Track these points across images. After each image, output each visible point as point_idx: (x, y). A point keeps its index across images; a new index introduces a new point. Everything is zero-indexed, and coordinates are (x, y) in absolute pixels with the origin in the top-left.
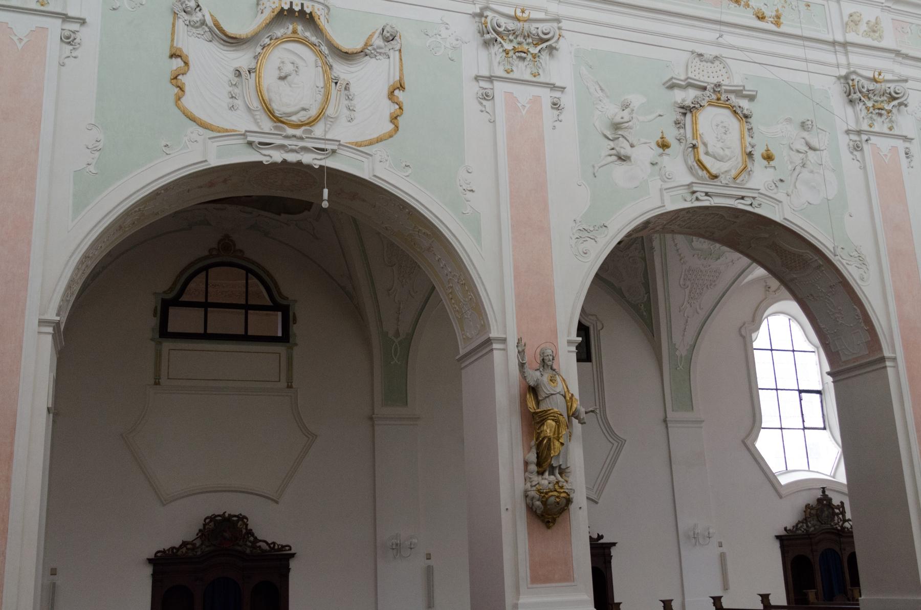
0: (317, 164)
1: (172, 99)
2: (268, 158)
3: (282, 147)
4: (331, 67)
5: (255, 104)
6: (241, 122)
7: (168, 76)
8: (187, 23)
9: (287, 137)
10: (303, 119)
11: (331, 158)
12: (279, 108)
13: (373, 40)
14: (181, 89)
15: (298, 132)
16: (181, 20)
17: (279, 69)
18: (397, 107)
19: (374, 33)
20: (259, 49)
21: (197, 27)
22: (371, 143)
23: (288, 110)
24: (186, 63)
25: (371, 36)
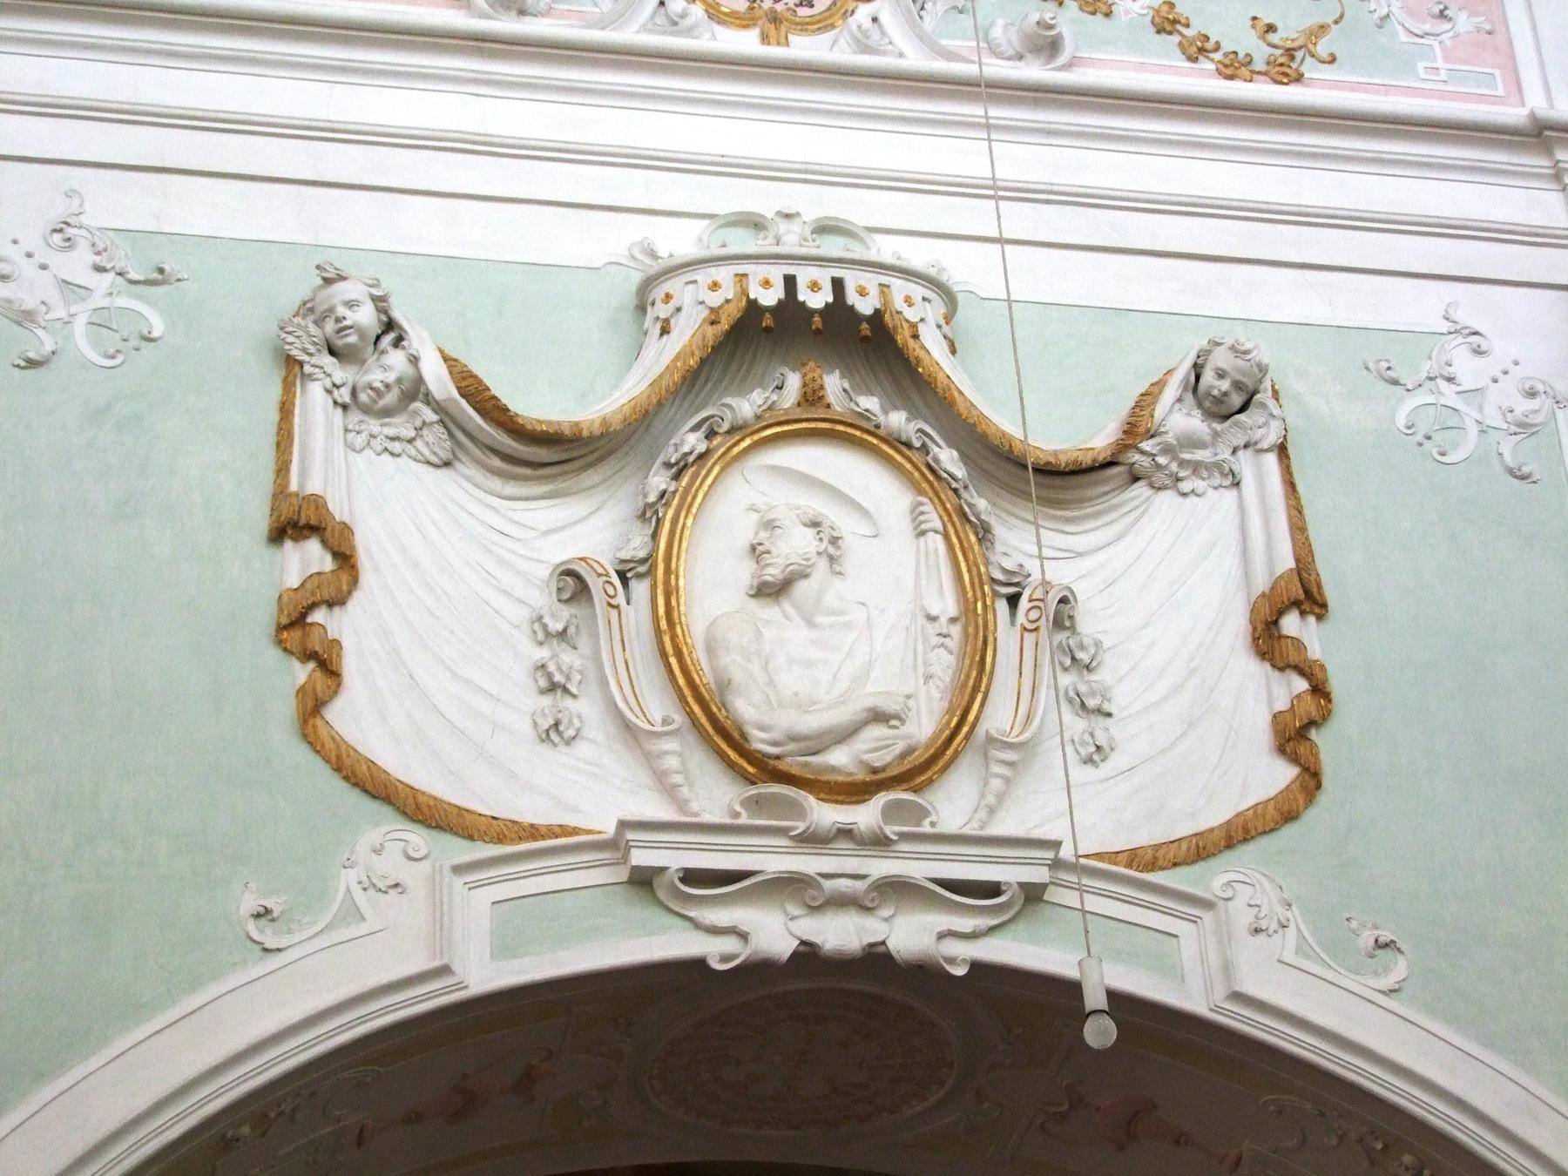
0: (960, 956)
1: (285, 709)
2: (729, 945)
3: (790, 886)
4: (984, 533)
5: (657, 706)
6: (596, 789)
7: (265, 615)
8: (344, 395)
9: (813, 840)
10: (879, 759)
11: (1020, 927)
12: (763, 715)
13: (1159, 412)
14: (326, 663)
15: (865, 816)
16: (316, 391)
17: (756, 552)
18: (1301, 685)
19: (1158, 387)
20: (659, 481)
21: (387, 413)
22: (1200, 849)
24: (345, 559)
25: (1148, 399)
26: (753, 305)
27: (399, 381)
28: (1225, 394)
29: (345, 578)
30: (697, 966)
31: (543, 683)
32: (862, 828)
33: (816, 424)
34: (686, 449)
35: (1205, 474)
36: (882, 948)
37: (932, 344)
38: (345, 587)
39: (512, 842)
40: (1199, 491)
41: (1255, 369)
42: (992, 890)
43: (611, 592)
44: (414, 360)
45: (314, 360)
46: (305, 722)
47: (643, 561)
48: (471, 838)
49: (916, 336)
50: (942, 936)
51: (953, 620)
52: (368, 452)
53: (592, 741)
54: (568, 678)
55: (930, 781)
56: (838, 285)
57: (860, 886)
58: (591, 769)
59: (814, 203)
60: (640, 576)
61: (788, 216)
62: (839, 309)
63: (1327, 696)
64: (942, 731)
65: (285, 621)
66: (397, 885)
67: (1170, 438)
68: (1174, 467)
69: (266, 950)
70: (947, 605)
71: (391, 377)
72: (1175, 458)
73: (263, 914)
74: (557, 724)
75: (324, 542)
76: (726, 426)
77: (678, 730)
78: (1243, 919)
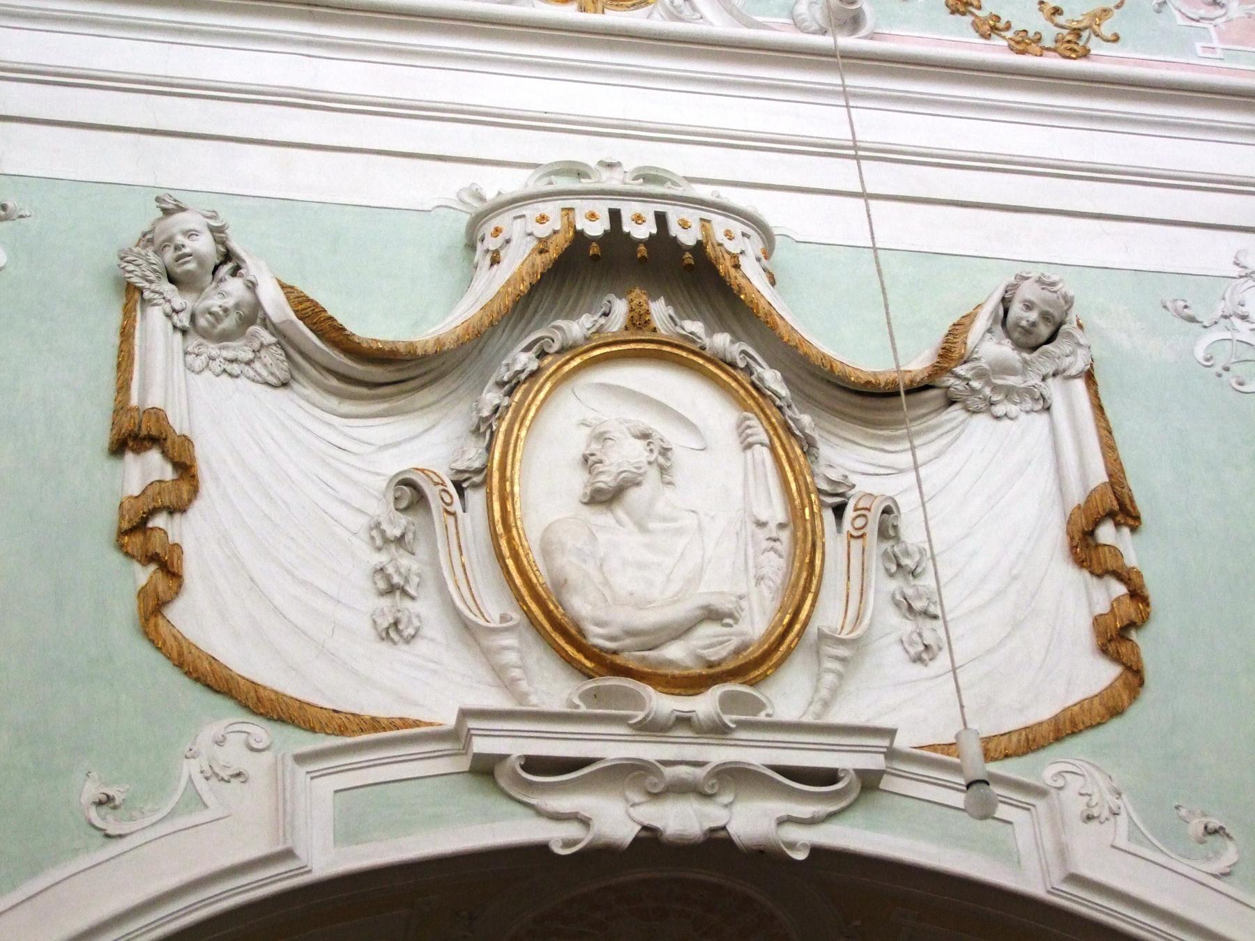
0: (800, 841)
1: (126, 609)
2: (571, 831)
4: (809, 446)
5: (494, 606)
6: (434, 683)
7: (107, 521)
9: (652, 728)
10: (714, 655)
11: (857, 815)
12: (599, 611)
14: (167, 565)
15: (704, 705)
16: (156, 315)
17: (588, 462)
18: (1120, 589)
20: (492, 397)
21: (225, 337)
22: (1031, 742)
23: (648, 618)
24: (185, 469)
25: (959, 328)
26: (579, 235)
27: (237, 306)
28: (1034, 324)
29: (185, 488)
30: (541, 850)
31: (382, 585)
32: (701, 716)
33: (642, 346)
34: (518, 367)
35: (1017, 399)
36: (722, 834)
37: (752, 274)
38: (185, 496)
39: (354, 733)
40: (1013, 415)
41: (1062, 301)
42: (830, 776)
43: (448, 500)
44: (252, 286)
45: (153, 287)
46: (147, 620)
47: (478, 471)
48: (312, 730)
49: (737, 266)
50: (782, 822)
51: (782, 526)
52: (207, 374)
53: (432, 640)
54: (407, 580)
55: (765, 676)
56: (661, 219)
57: (700, 773)
58: (432, 665)
59: (636, 155)
60: (475, 486)
61: (610, 166)
62: (663, 238)
63: (1145, 600)
64: (774, 628)
65: (126, 526)
66: (239, 775)
67: (983, 364)
68: (987, 391)
69: (108, 836)
70: (775, 511)
71: (230, 302)
72: (988, 383)
73: (105, 802)
74: (396, 624)
75: (165, 453)
76: (556, 347)
77: (517, 626)
78: (1076, 807)
